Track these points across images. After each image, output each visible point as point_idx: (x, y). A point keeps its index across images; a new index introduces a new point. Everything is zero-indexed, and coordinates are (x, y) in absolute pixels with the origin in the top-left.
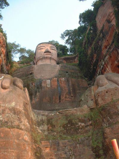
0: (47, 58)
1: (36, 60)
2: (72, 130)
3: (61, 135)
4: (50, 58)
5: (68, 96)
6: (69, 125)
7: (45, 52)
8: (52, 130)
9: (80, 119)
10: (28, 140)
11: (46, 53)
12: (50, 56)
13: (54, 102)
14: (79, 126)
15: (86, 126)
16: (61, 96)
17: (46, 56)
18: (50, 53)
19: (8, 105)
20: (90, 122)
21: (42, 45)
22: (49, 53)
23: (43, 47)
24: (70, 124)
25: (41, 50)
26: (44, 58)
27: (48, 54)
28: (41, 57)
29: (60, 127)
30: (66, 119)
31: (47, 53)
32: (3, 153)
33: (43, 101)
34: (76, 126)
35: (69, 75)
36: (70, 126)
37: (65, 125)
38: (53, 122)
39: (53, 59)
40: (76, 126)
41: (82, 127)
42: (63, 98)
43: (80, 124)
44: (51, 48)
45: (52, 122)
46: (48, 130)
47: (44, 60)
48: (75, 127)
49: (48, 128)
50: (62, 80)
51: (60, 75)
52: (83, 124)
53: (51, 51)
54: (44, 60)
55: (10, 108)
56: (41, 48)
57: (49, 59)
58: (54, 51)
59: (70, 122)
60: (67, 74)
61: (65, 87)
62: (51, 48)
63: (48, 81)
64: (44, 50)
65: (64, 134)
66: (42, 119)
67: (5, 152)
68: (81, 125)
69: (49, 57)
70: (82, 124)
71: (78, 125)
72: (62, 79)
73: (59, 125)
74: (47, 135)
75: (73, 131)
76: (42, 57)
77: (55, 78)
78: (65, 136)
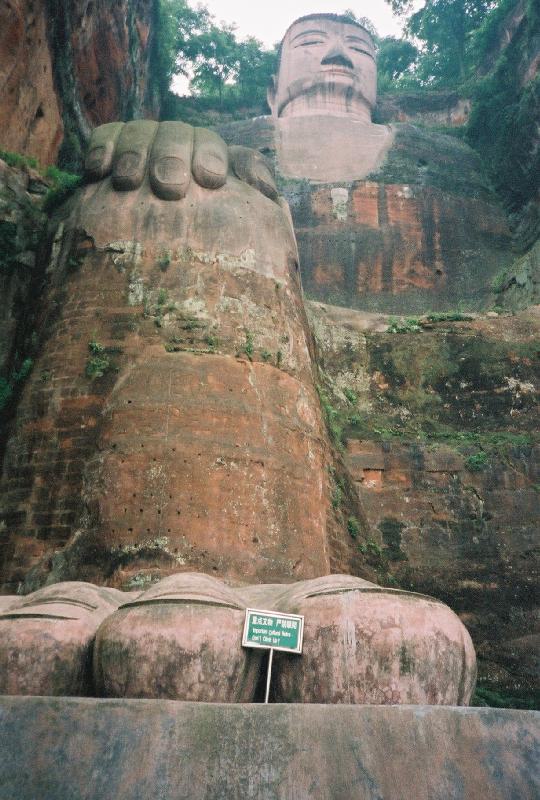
0: (332, 86)
1: (282, 95)
2: (478, 406)
3: (432, 421)
4: (349, 93)
5: (420, 269)
6: (464, 385)
7: (325, 62)
8: (389, 397)
9: (517, 364)
10: (311, 421)
12: (346, 81)
13: (360, 289)
14: (508, 394)
16: (391, 263)
17: (329, 79)
18: (347, 69)
19: (226, 259)
21: (311, 25)
22: (342, 68)
23: (319, 37)
24: (467, 381)
25: (310, 48)
26: (322, 86)
27: (340, 71)
28: (305, 80)
29: (425, 385)
30: (453, 358)
31: (335, 67)
32: (220, 464)
33: (312, 278)
35: (429, 173)
36: (468, 389)
37: (447, 379)
38: (397, 363)
39: (361, 97)
40: (498, 391)
41: (523, 396)
42: (399, 272)
43: (512, 382)
44: (354, 44)
45: (391, 362)
46: (372, 394)
47: (319, 97)
48: (493, 394)
49: (374, 385)
50: (400, 194)
51: (388, 176)
53: (354, 57)
54: (319, 97)
55: (239, 271)
56: (310, 38)
57: (340, 94)
59: (468, 370)
60: (425, 169)
61: (409, 228)
62: (354, 44)
63: (341, 195)
64: (322, 52)
65: (444, 419)
66: (349, 345)
67: (229, 460)
68: (518, 388)
69: (339, 84)
70: (522, 386)
71: (505, 389)
72: (402, 190)
73: (423, 379)
74: (372, 416)
75: (482, 410)
76: (309, 84)
77: (368, 185)
78: (448, 429)
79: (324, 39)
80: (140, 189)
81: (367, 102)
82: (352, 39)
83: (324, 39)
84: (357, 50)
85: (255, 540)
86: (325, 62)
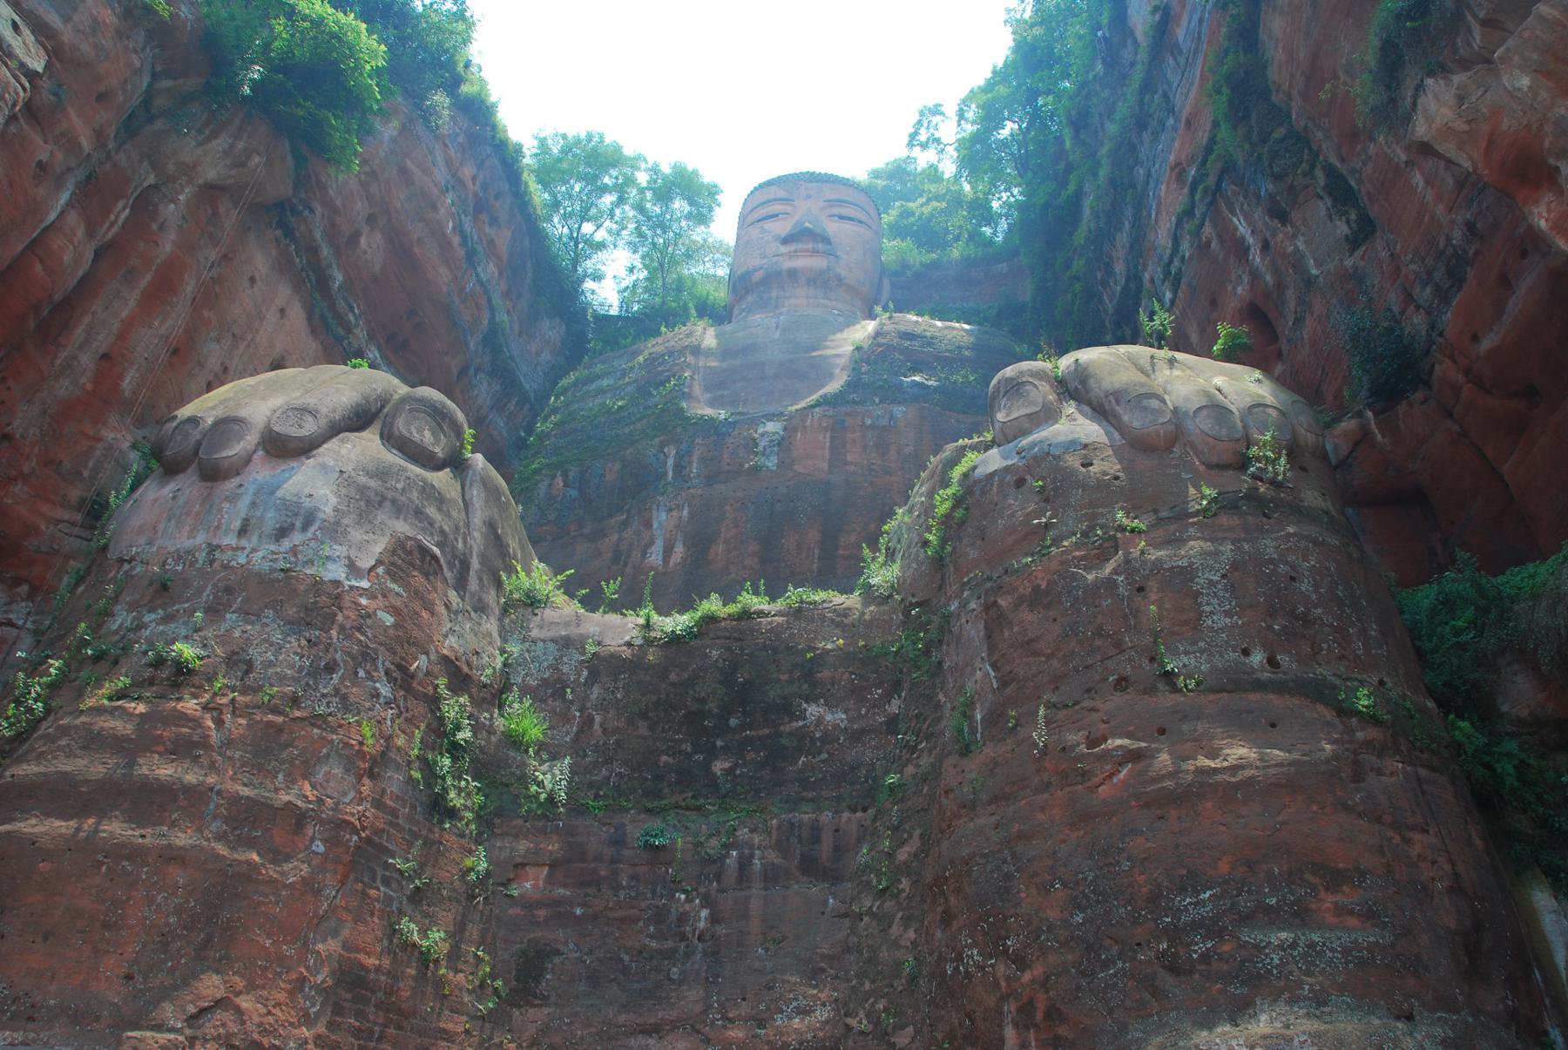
0: (793, 274)
7: (786, 241)
11: (793, 247)
14: (801, 736)
15: (857, 737)
17: (788, 264)
20: (894, 707)
22: (810, 246)
25: (768, 225)
26: (778, 273)
34: (787, 728)
40: (787, 728)
43: (813, 710)
44: (835, 211)
52: (836, 717)
53: (833, 228)
58: (847, 227)
76: (758, 276)
79: (789, 209)
80: (190, 471)
81: (850, 289)
82: (831, 203)
83: (789, 209)
84: (841, 217)
85: (129, 977)
86: (786, 241)
